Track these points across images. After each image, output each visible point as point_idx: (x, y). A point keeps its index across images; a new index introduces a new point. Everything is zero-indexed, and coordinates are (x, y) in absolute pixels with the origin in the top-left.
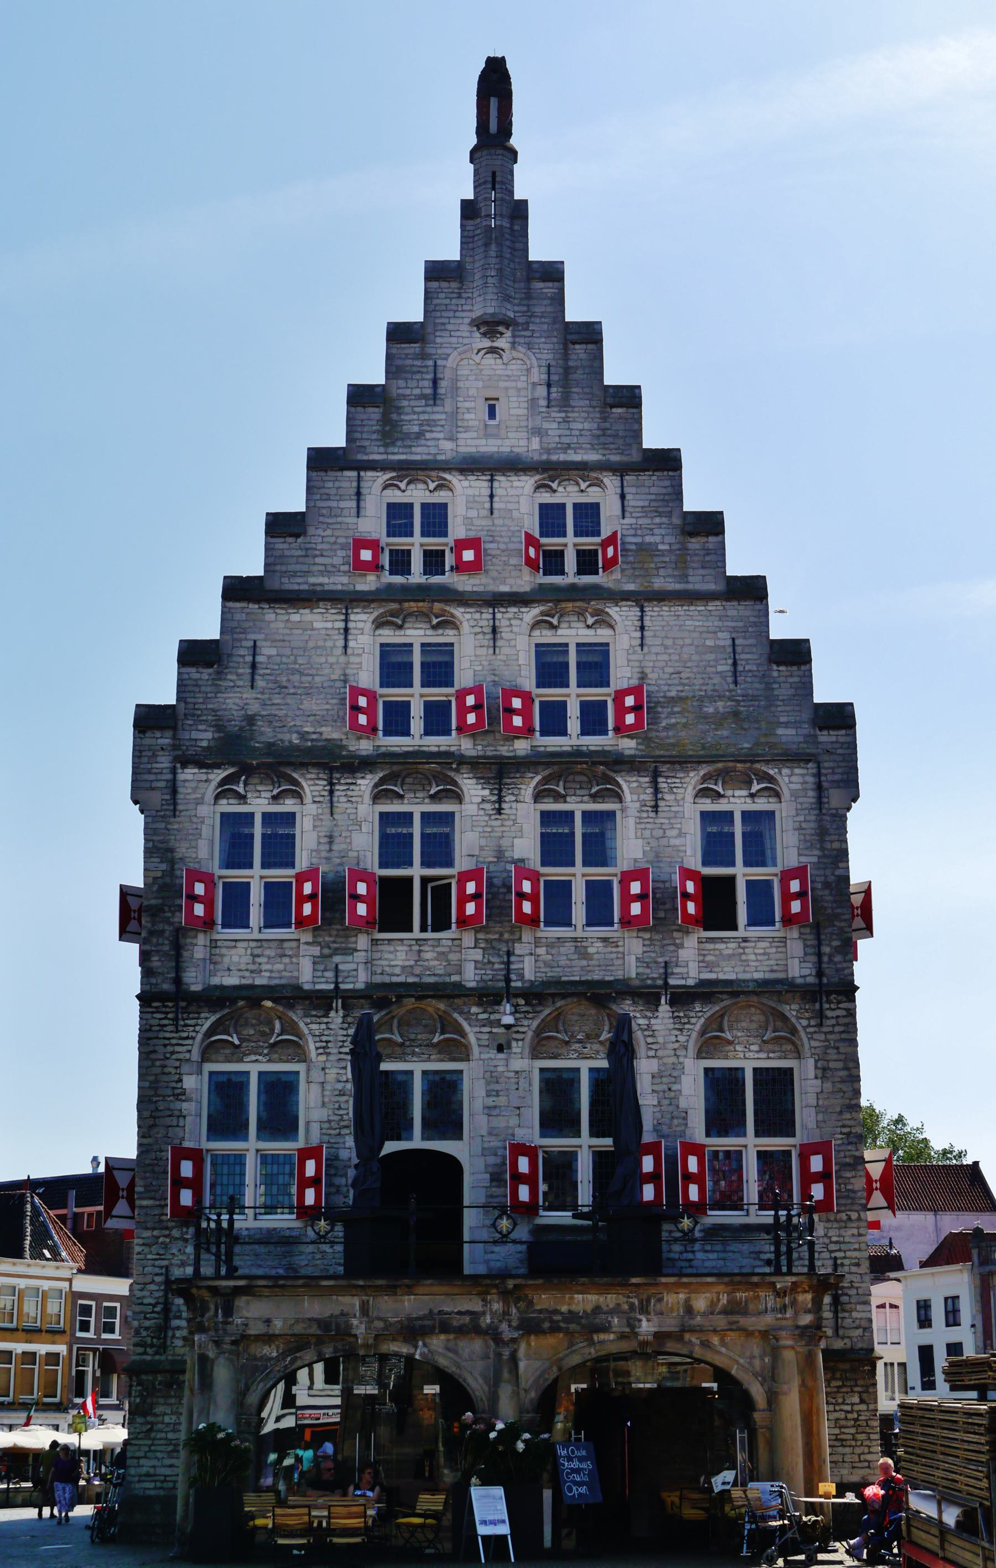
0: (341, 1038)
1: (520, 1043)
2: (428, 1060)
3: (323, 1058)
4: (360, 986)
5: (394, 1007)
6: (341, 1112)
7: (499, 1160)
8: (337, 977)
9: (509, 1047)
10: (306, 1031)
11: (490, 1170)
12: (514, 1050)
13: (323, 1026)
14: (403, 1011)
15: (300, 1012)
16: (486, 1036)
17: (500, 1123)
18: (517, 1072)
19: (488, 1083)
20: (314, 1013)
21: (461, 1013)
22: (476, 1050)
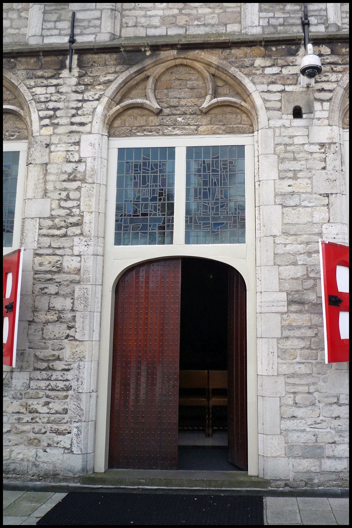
0: (74, 105)
1: (326, 105)
2: (196, 132)
3: (49, 130)
4: (103, 38)
5: (148, 62)
6: (69, 204)
7: (299, 272)
8: (73, 27)
9: (311, 111)
10: (28, 96)
11: (287, 286)
12: (318, 114)
13: (52, 90)
14: (160, 69)
15: (21, 73)
16: (278, 96)
17: (299, 217)
18: (322, 145)
19: (282, 160)
20: (40, 73)
21: (241, 67)
22: (263, 115)
